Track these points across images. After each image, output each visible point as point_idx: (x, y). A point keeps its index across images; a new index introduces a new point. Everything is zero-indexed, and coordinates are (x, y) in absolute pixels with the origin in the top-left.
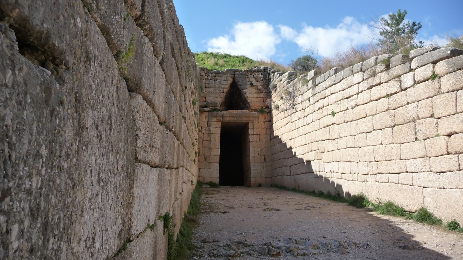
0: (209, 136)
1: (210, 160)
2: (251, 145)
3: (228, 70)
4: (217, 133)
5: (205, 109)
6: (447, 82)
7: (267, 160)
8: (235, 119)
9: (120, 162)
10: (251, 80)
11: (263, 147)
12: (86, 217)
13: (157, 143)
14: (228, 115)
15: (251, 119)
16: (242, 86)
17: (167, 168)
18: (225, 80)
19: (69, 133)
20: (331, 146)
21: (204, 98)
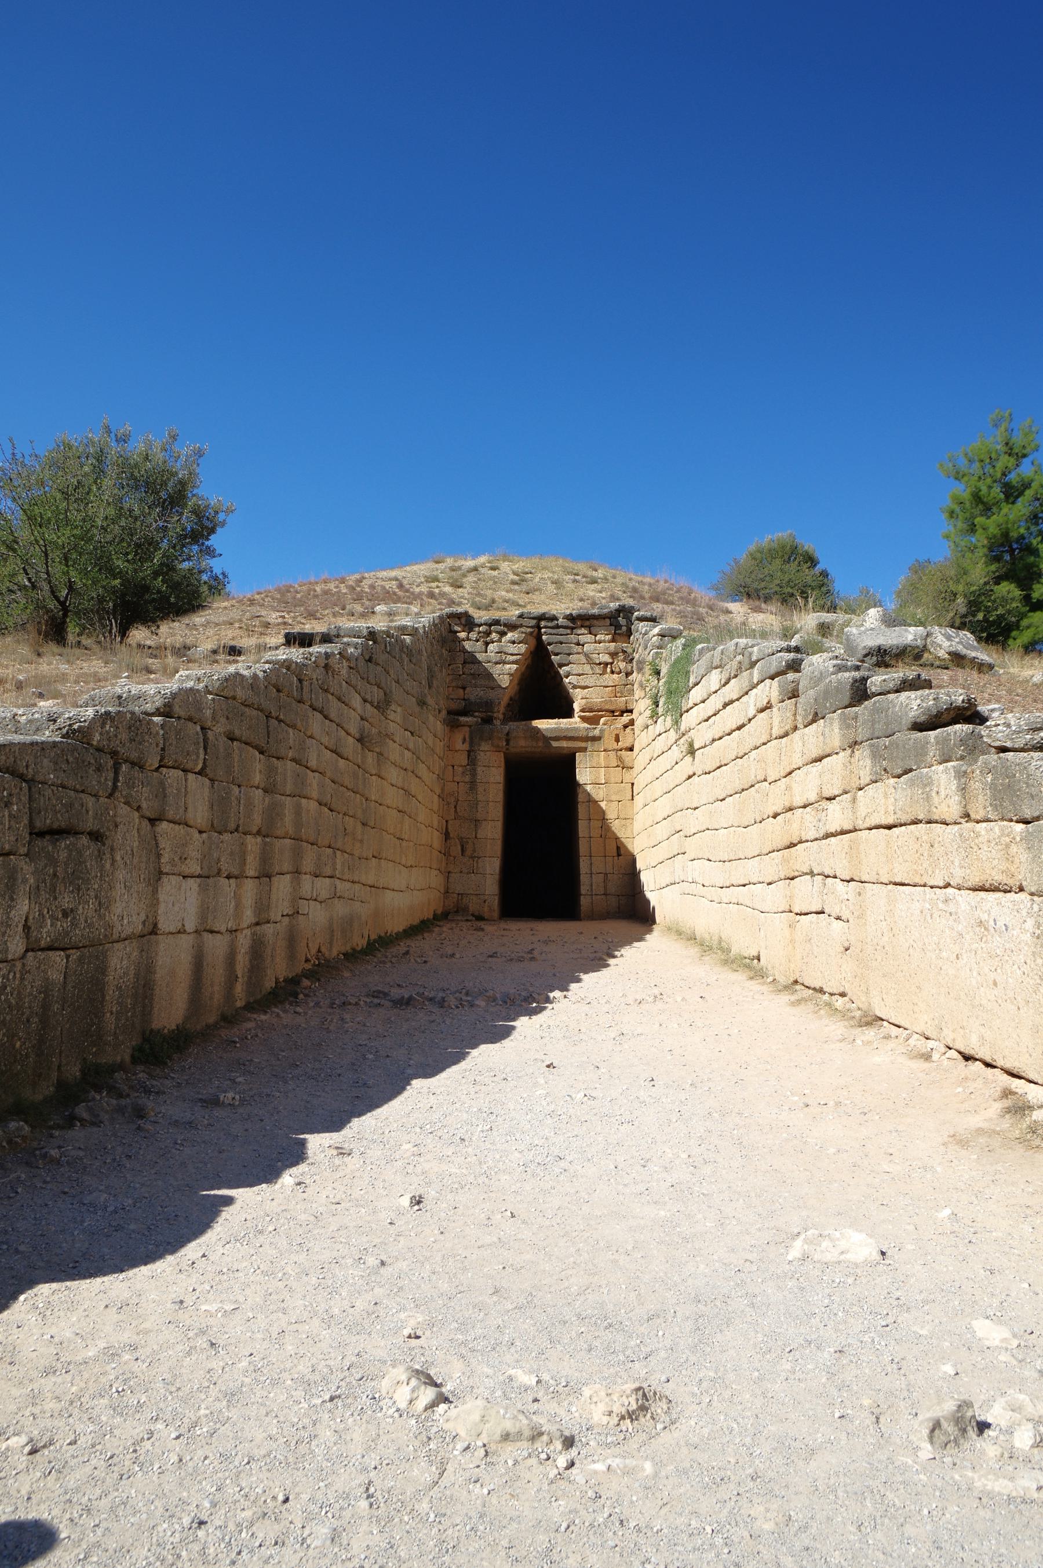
1: (474, 851)
3: (521, 616)
5: (463, 719)
6: (778, 718)
9: (142, 876)
10: (582, 639)
12: (117, 905)
13: (195, 854)
15: (583, 745)
17: (228, 877)
18: (514, 642)
19: (108, 866)
20: (693, 821)
21: (461, 691)
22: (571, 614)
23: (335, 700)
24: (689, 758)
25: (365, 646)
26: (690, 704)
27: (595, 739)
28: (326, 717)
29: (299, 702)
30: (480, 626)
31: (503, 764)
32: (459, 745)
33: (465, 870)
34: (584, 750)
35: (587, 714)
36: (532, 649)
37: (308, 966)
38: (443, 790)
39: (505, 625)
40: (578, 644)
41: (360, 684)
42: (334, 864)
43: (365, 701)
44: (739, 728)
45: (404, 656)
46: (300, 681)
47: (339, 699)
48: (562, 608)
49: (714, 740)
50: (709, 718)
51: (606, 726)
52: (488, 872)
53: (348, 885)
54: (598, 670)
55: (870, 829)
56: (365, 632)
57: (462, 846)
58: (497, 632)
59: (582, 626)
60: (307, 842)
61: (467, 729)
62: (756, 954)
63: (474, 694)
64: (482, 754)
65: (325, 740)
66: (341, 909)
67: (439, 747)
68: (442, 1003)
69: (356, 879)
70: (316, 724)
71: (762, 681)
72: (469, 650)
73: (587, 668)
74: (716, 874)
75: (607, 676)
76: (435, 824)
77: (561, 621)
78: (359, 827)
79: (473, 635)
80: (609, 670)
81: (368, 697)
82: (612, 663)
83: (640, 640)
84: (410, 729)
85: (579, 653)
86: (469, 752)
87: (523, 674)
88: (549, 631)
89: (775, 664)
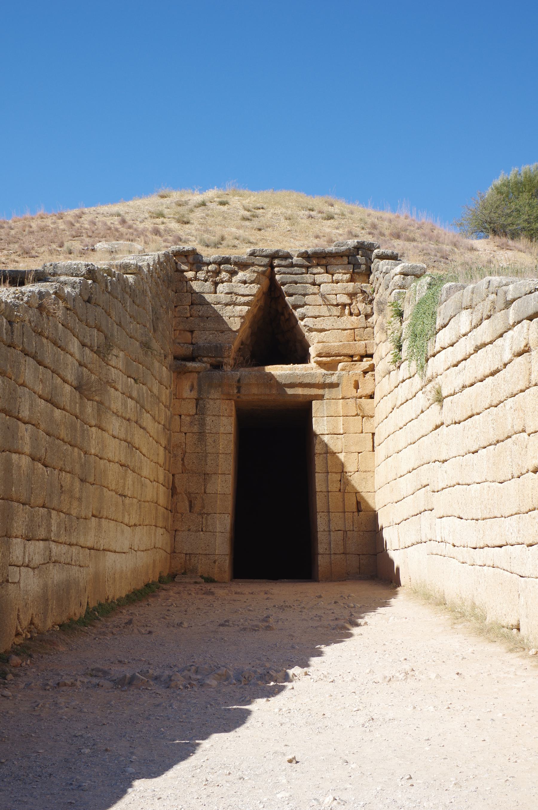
1: (203, 507)
4: (222, 430)
5: (190, 364)
10: (319, 279)
16: (293, 298)
18: (245, 282)
20: (441, 476)
21: (189, 334)
22: (306, 252)
23: (50, 345)
24: (436, 407)
25: (84, 285)
26: (438, 348)
28: (40, 363)
29: (9, 346)
31: (234, 413)
32: (187, 393)
34: (321, 397)
35: (324, 359)
36: (265, 289)
37: (19, 640)
38: (169, 441)
39: (236, 264)
40: (314, 284)
41: (78, 327)
42: (49, 525)
43: (84, 345)
44: (493, 374)
45: (127, 296)
46: (10, 323)
47: (55, 343)
48: (296, 246)
49: (464, 387)
50: (459, 362)
51: (346, 373)
52: (218, 530)
53: (64, 548)
54: (336, 311)
56: (84, 270)
57: (190, 502)
58: (227, 271)
59: (318, 265)
60: (18, 502)
61: (195, 375)
62: (515, 623)
63: (203, 338)
64: (211, 402)
65: (39, 388)
66: (56, 575)
67: (165, 395)
68: (168, 683)
69: (74, 541)
70: (28, 371)
71: (519, 322)
72: (197, 290)
73: (324, 310)
74: (469, 533)
75: (344, 318)
76: (161, 478)
77: (296, 260)
78: (77, 483)
79: (201, 275)
80: (347, 311)
81: (87, 341)
82: (350, 305)
83: (381, 279)
84: (133, 376)
85: (314, 294)
87: (255, 316)
88: (283, 269)
89: (533, 303)
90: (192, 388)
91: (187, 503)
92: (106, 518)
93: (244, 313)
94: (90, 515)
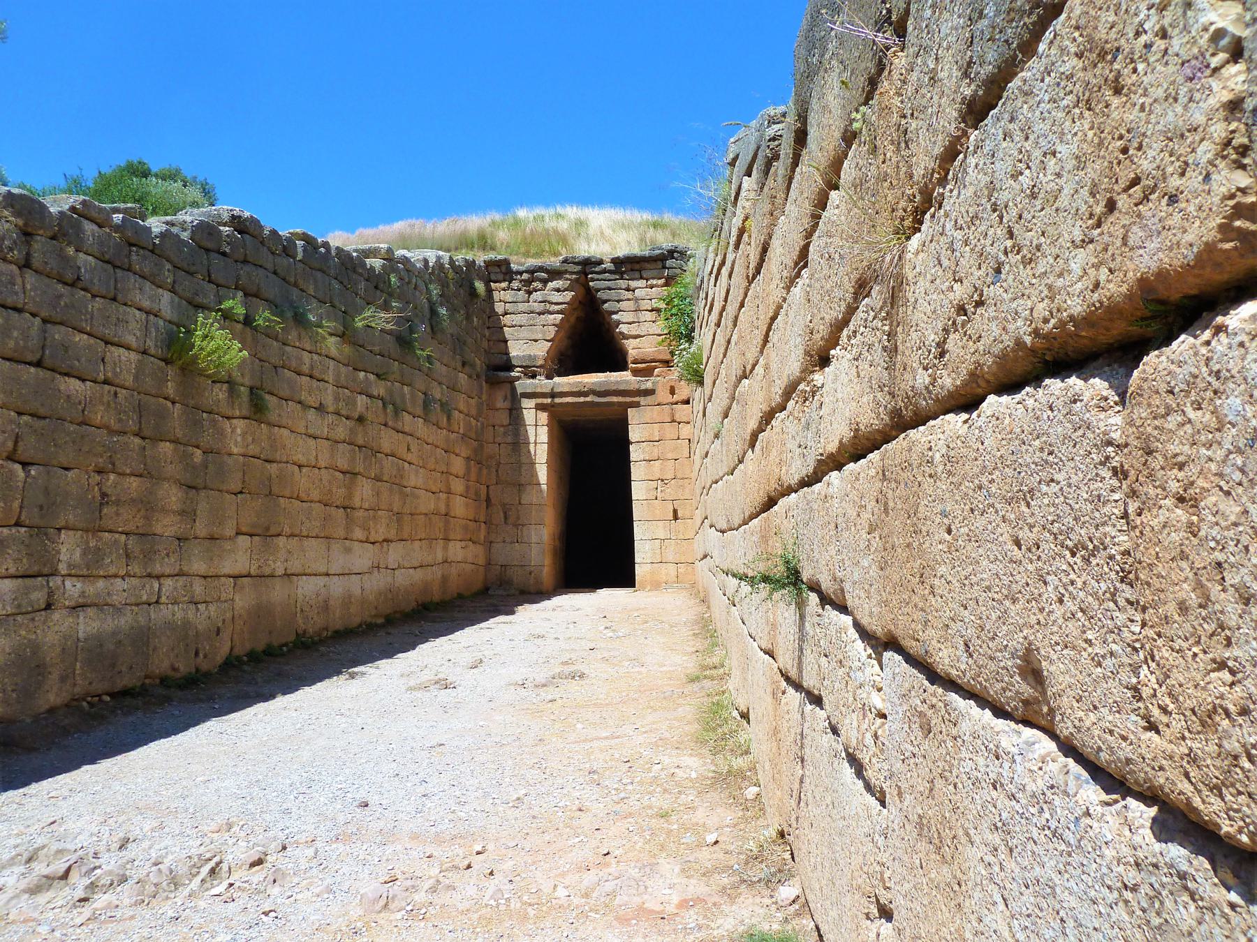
0: (514, 450)
1: (518, 518)
2: (637, 472)
3: (565, 261)
7: (680, 515)
8: (588, 399)
11: (670, 476)
14: (566, 389)
18: (558, 290)
27: (650, 392)
30: (521, 273)
32: (500, 404)
33: (508, 540)
34: (637, 405)
40: (628, 289)
54: (649, 316)
55: (967, 402)
57: (505, 513)
86: (510, 410)
90: (505, 399)
91: (502, 515)
92: (292, 535)
93: (558, 322)
94: (230, 532)
